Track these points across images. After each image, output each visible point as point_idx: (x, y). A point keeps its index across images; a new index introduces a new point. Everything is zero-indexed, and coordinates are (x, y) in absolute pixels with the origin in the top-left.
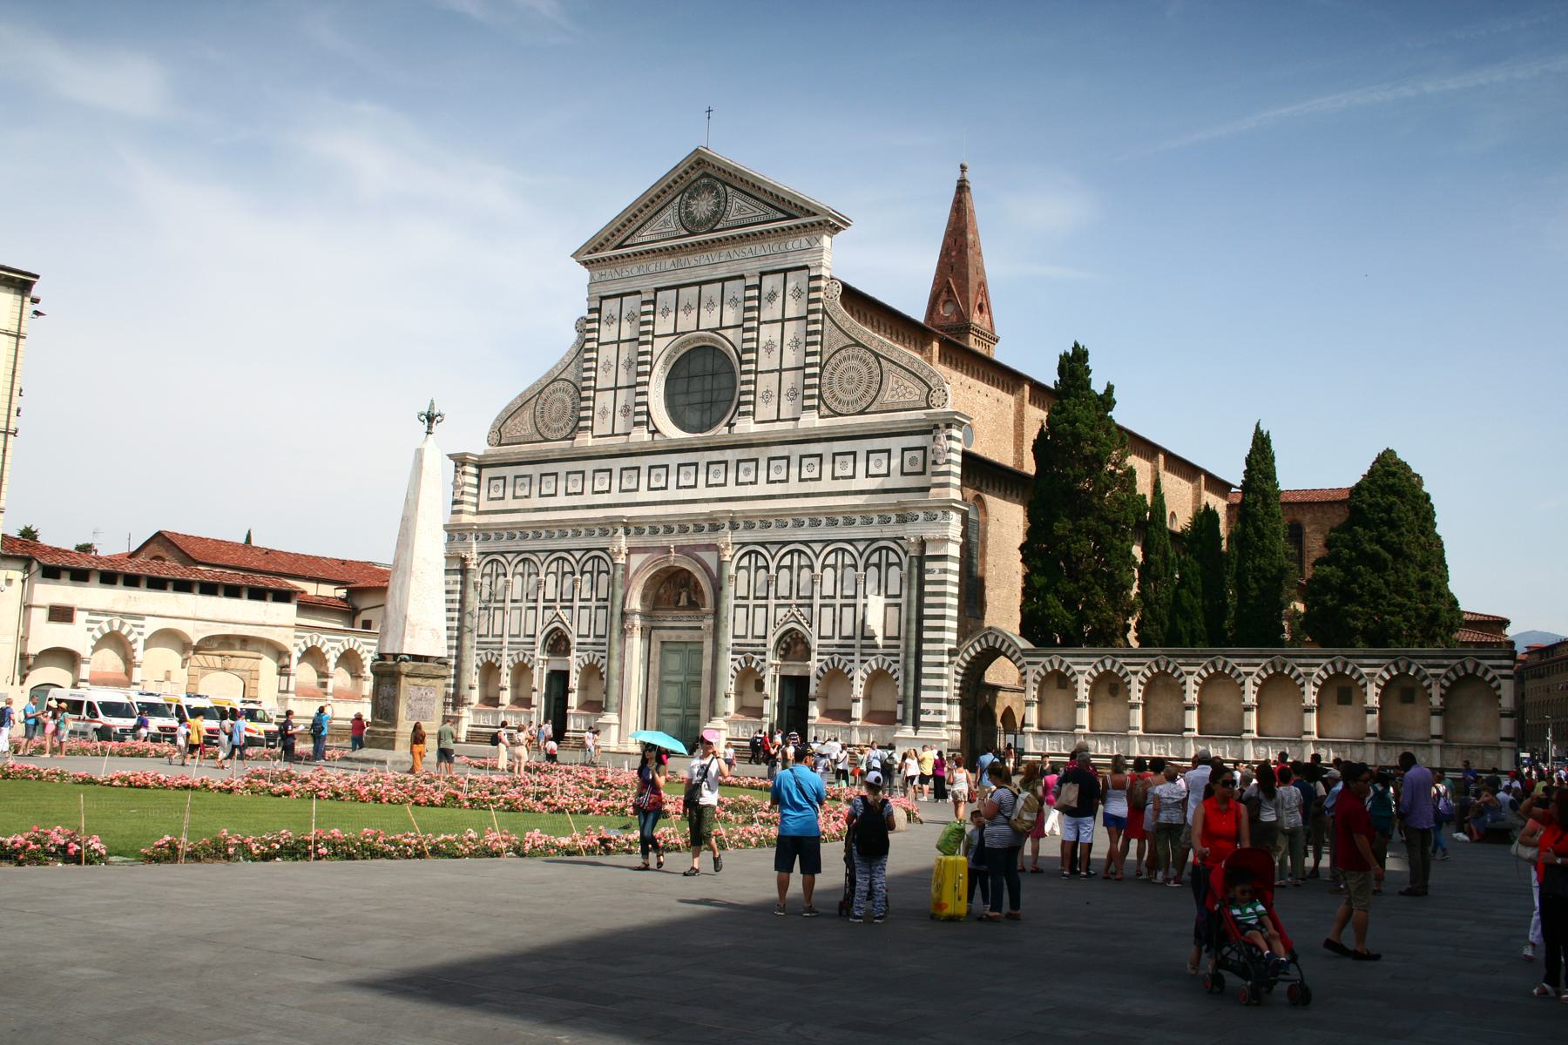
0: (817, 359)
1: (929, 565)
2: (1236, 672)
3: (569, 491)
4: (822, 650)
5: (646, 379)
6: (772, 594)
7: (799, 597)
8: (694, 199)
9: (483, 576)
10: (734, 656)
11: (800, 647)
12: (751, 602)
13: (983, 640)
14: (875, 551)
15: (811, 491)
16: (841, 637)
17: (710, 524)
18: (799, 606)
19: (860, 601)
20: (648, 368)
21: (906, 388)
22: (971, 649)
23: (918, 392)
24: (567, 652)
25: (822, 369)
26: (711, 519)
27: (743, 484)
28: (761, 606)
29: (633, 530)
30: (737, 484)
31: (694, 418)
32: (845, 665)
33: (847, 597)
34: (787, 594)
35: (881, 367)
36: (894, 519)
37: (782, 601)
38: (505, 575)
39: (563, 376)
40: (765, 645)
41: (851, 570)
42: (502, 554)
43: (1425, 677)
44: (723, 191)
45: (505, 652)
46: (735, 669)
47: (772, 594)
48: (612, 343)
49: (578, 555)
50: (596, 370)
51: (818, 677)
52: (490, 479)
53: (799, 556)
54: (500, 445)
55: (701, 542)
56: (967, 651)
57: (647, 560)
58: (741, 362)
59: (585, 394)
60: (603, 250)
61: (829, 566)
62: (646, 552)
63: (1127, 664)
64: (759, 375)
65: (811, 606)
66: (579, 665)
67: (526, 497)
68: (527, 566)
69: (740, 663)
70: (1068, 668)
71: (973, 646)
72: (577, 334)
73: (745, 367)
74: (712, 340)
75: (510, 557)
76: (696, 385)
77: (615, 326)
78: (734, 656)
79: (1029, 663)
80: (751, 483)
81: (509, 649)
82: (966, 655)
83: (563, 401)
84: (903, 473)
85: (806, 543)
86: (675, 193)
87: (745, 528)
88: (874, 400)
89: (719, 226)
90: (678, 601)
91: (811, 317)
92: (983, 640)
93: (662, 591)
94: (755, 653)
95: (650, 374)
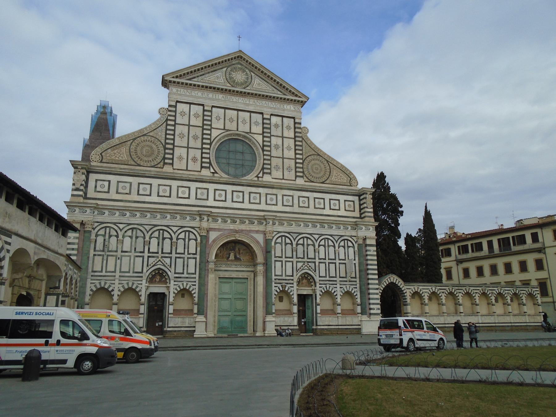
0: (300, 157)
1: (368, 248)
2: (472, 292)
3: (160, 195)
4: (321, 282)
5: (208, 146)
6: (295, 256)
7: (308, 258)
8: (234, 72)
9: (97, 235)
10: (276, 285)
11: (305, 281)
12: (284, 259)
13: (389, 279)
14: (342, 240)
15: (305, 212)
16: (330, 277)
17: (258, 221)
18: (308, 262)
19: (338, 262)
20: (208, 141)
21: (341, 177)
22: (384, 283)
23: (346, 179)
24: (166, 283)
25: (303, 161)
26: (259, 219)
27: (269, 204)
28: (289, 261)
29: (210, 219)
30: (266, 204)
31: (232, 170)
32: (332, 289)
33: (331, 259)
34: (302, 256)
35: (329, 166)
36: (350, 228)
37: (300, 260)
38: (117, 236)
39: (151, 134)
40: (293, 280)
41: (333, 248)
42: (115, 224)
43: (521, 294)
44: (249, 74)
45: (117, 282)
46: (276, 291)
47: (295, 256)
48: (184, 124)
49: (175, 229)
50: (174, 135)
51: (320, 295)
52: (96, 181)
53: (307, 240)
54: (101, 162)
55: (254, 229)
56: (383, 284)
57: (220, 235)
58: (263, 150)
59: (168, 146)
60: (181, 79)
61: (322, 245)
62: (220, 231)
63: (440, 289)
64: (272, 158)
65: (315, 263)
66: (176, 289)
67: (127, 193)
68: (134, 233)
69: (279, 288)
70: (421, 290)
71: (385, 282)
72: (158, 116)
73: (265, 153)
74: (244, 137)
75: (121, 226)
76: (232, 156)
77: (186, 117)
78: (276, 285)
79: (407, 289)
80: (274, 205)
81: (119, 280)
82: (383, 285)
83: (151, 147)
84: (345, 210)
85: (311, 234)
86: (223, 66)
87: (279, 225)
88: (328, 179)
89: (247, 88)
90: (229, 257)
91: (297, 139)
92: (389, 279)
93: (219, 252)
94: (287, 284)
95: (210, 144)
